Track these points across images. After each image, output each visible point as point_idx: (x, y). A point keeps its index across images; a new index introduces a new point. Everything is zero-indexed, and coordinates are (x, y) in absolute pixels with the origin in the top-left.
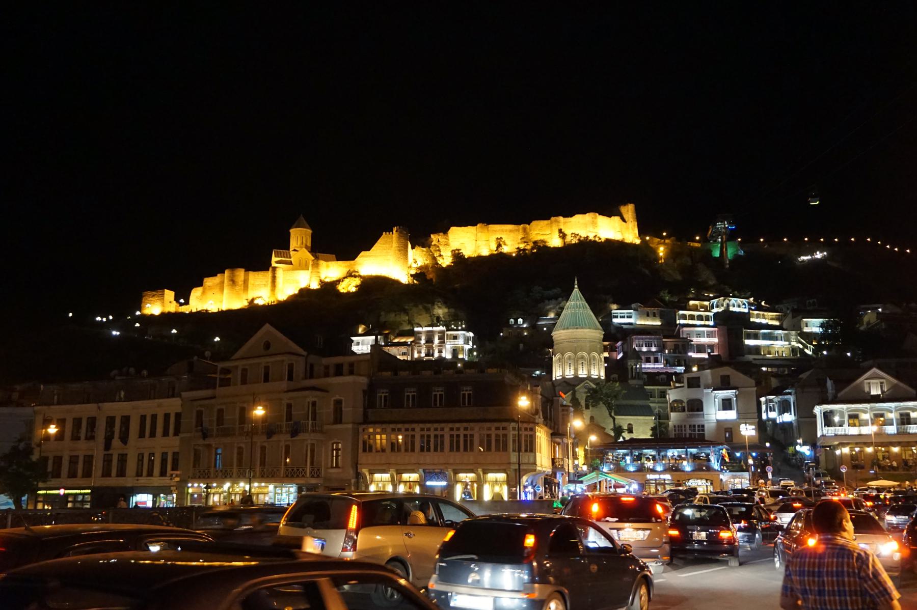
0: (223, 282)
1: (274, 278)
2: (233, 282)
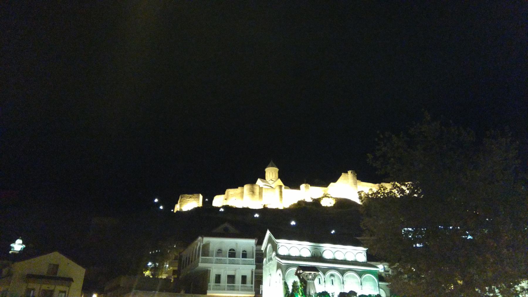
0: (243, 192)
1: (281, 192)
2: (253, 192)
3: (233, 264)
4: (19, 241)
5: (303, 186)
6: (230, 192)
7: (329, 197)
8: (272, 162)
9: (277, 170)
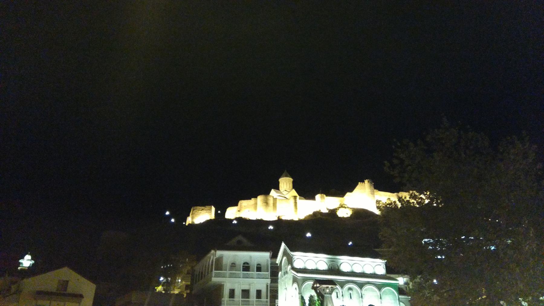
0: (256, 204)
1: (296, 203)
2: (266, 203)
3: (247, 278)
4: (28, 257)
5: (318, 197)
6: (243, 203)
7: (345, 208)
8: (286, 172)
9: (291, 180)
